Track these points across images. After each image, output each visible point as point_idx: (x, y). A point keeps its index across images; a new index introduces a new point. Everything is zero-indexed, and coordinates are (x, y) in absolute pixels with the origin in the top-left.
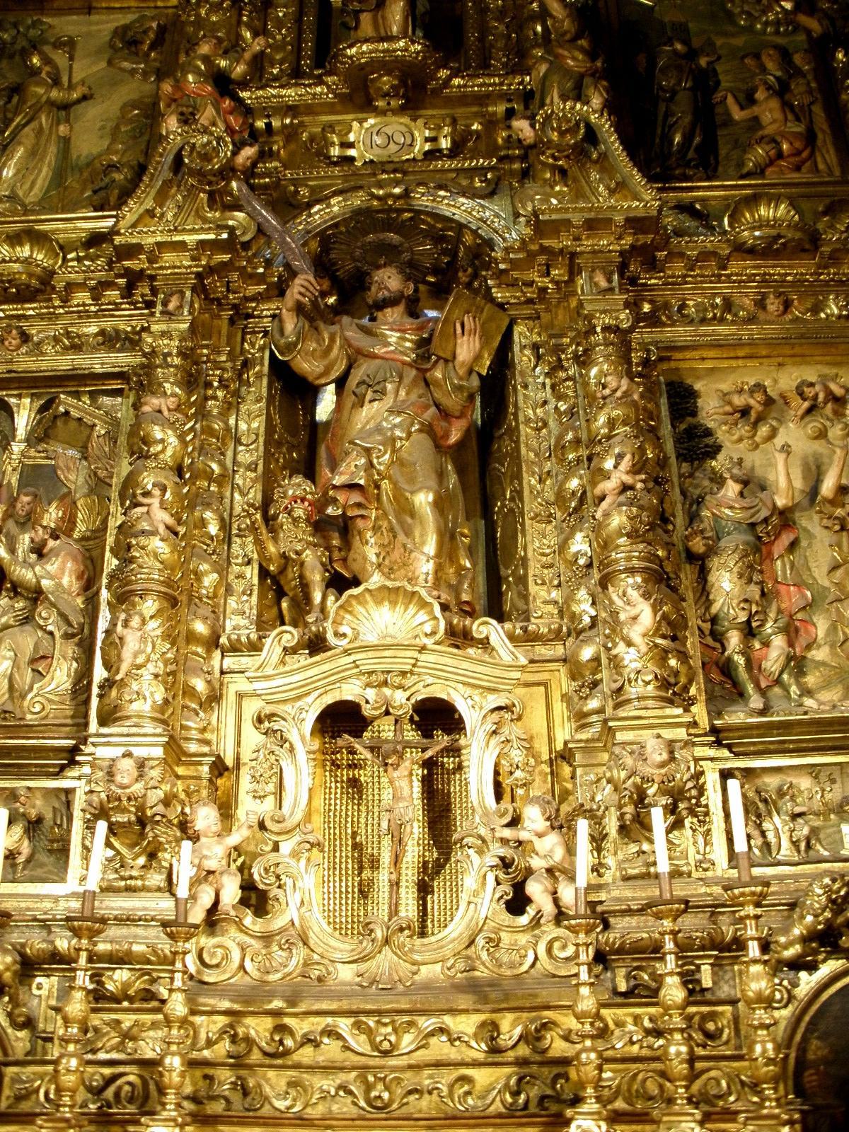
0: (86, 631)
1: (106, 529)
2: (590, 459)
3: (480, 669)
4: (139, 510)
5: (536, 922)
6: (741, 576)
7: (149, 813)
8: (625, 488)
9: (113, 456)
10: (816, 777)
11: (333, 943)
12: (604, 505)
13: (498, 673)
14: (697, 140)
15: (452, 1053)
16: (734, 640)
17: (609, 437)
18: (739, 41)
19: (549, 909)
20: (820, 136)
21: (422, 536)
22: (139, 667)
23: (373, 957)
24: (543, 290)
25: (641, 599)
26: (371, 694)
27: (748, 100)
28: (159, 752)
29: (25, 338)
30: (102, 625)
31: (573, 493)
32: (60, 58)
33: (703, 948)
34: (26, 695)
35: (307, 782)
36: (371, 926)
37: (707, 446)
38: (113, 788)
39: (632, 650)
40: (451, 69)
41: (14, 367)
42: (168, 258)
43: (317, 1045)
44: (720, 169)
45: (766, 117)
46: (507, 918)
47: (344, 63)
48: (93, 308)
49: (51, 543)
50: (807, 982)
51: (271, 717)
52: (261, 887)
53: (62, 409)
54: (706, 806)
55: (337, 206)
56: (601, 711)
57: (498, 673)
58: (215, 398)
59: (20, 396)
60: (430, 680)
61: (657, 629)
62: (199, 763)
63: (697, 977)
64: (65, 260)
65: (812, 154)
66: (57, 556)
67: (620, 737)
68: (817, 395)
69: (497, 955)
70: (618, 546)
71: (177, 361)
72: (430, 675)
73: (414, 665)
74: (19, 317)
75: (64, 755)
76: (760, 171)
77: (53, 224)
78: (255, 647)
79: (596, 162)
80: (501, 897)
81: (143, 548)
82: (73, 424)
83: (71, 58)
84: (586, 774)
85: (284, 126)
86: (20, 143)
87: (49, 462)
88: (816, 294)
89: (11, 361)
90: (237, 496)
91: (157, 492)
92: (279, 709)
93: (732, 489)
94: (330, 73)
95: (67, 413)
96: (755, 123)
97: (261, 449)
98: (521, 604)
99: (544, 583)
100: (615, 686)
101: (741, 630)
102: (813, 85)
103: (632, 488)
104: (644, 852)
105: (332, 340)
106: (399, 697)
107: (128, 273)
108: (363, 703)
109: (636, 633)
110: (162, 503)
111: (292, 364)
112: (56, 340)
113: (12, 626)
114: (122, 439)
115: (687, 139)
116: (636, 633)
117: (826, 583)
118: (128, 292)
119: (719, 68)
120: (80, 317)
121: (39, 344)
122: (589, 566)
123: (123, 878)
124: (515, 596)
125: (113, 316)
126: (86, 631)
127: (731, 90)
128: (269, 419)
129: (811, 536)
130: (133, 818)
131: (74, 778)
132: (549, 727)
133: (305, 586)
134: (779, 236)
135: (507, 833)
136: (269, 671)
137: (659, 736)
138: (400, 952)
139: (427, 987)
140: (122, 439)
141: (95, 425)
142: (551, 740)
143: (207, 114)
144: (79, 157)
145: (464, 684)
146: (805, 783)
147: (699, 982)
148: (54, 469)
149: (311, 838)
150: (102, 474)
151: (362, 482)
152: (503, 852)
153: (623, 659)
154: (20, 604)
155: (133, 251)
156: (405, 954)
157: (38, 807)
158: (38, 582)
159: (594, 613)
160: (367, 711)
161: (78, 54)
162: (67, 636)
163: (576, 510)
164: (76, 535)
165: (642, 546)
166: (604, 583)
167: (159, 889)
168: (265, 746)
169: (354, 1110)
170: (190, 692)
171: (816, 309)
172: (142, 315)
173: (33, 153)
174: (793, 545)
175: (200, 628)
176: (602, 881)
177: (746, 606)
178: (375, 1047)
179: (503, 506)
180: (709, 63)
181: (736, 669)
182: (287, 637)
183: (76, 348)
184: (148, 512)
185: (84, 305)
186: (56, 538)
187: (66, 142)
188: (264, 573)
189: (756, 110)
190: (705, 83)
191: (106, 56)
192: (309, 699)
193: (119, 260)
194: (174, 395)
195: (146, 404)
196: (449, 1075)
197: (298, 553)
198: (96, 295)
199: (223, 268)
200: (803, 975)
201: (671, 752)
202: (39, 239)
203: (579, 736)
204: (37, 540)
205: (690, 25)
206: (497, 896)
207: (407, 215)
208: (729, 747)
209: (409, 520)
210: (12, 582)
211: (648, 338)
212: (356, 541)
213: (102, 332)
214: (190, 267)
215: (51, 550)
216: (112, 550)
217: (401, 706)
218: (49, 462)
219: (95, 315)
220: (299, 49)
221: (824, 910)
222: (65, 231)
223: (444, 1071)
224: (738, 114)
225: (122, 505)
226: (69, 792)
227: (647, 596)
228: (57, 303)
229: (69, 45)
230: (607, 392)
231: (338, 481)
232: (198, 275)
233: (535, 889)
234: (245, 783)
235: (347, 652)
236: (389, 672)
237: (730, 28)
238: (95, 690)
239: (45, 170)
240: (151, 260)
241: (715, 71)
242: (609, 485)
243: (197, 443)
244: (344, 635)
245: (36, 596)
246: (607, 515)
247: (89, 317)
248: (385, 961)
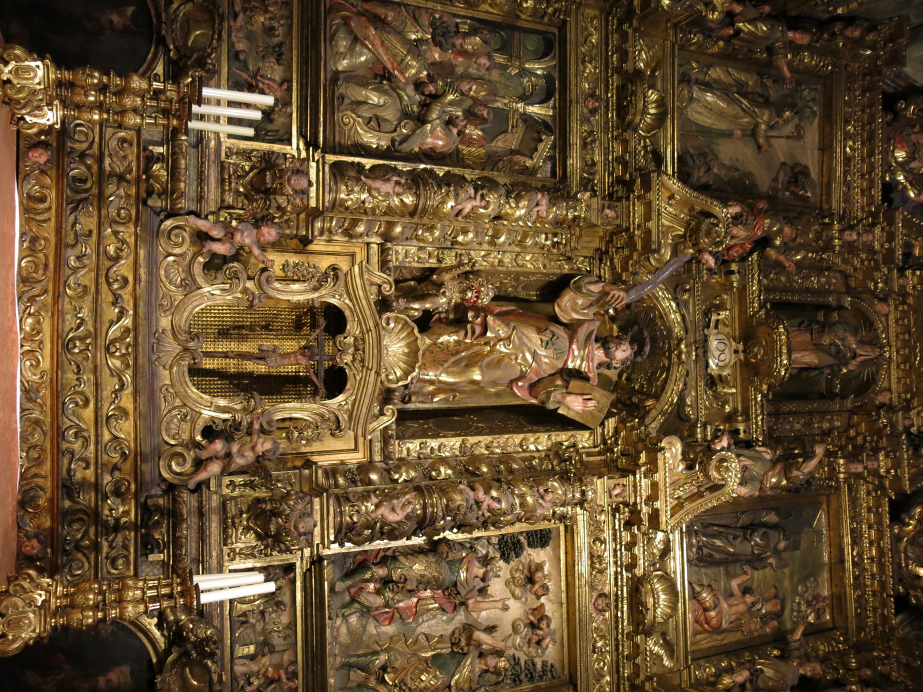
0: (397, 154)
1: (464, 167)
2: (499, 481)
3: (364, 410)
4: (472, 192)
5: (197, 445)
6: (423, 576)
7: (271, 197)
9: (512, 172)
10: (288, 627)
11: (186, 314)
12: (468, 490)
13: (362, 421)
14: (717, 556)
15: (106, 393)
16: (381, 572)
18: (786, 583)
19: (204, 455)
20: (720, 637)
21: (453, 372)
22: (369, 192)
23: (175, 340)
25: (405, 514)
26: (350, 340)
28: (313, 203)
29: (593, 111)
30: (401, 165)
31: (478, 469)
32: (789, 129)
33: (174, 555)
34: (354, 113)
35: (296, 298)
36: (196, 339)
37: (509, 554)
38: (289, 174)
39: (373, 507)
40: (768, 394)
41: (574, 105)
42: (639, 209)
43: (114, 304)
44: (696, 569)
46: (200, 425)
47: (773, 322)
48: (610, 157)
49: (455, 131)
50: (151, 624)
51: (336, 277)
52: (225, 268)
53: (544, 137)
54: (271, 555)
55: (675, 317)
56: (337, 485)
57: (362, 421)
58: (546, 239)
59: (554, 108)
60: (358, 378)
61: (386, 524)
62: (307, 230)
63: (156, 551)
64: (645, 138)
65: (706, 631)
66: (446, 135)
67: (317, 501)
68: (541, 629)
69: (175, 420)
70: (441, 499)
71: (570, 216)
72: (361, 378)
73: (368, 368)
74: (607, 107)
75: (313, 139)
77: (671, 129)
78: (384, 265)
80: (214, 423)
81: (447, 194)
82: (533, 146)
83: (788, 137)
84: (295, 477)
85: (732, 283)
86: (728, 104)
87: (510, 128)
89: (577, 102)
90: (483, 253)
91: (483, 203)
92: (341, 282)
94: (767, 314)
95: (541, 141)
97: (513, 269)
98: (409, 432)
99: (421, 448)
100: (351, 496)
101: (387, 576)
102: (756, 634)
103: (479, 508)
104: (241, 515)
105: (583, 314)
106: (348, 359)
107: (633, 181)
108: (345, 335)
109: (384, 511)
110: (476, 206)
111: (568, 290)
112: (591, 133)
113: (401, 103)
114: (522, 178)
115: (718, 549)
116: (384, 511)
118: (620, 181)
119: (768, 570)
120: (605, 148)
121: (589, 121)
122: (431, 478)
123: (230, 176)
124: (415, 429)
125: (605, 171)
126: (397, 154)
127: (752, 578)
128: (533, 274)
130: (268, 186)
131: (298, 145)
132: (328, 451)
133: (422, 297)
135: (256, 426)
136: (366, 276)
137: (315, 526)
138: (179, 358)
139: (154, 375)
140: (522, 178)
141: (532, 159)
142: (320, 453)
143: (740, 232)
144: (718, 144)
145: (355, 400)
146: (285, 619)
147: (152, 552)
148: (505, 132)
149: (256, 301)
150: (500, 165)
151: (489, 334)
152: (245, 423)
153: (368, 502)
154: (415, 109)
155: (647, 186)
156: (177, 361)
157: (279, 120)
158: (429, 122)
160: (340, 338)
161: (791, 142)
162: (393, 140)
163: (467, 470)
164: (460, 146)
165: (441, 514)
166: (418, 489)
167: (223, 201)
168: (318, 272)
169: (67, 329)
170: (355, 223)
172: (605, 190)
173: (721, 114)
175: (398, 229)
176: (224, 488)
177: (402, 580)
178: (113, 342)
179: (473, 421)
180: (771, 564)
182: (387, 287)
183: (584, 145)
184: (470, 198)
185: (613, 152)
186: (459, 134)
187: (729, 135)
188: (432, 271)
190: (756, 561)
191: (789, 162)
192: (347, 301)
193: (641, 176)
194: (548, 216)
195: (543, 195)
196: (89, 390)
197: (444, 293)
198: (620, 160)
199: (631, 244)
200: (155, 620)
201: (305, 534)
202: (660, 119)
203: (320, 472)
204: (457, 121)
205: (798, 552)
206: (216, 421)
207: (667, 363)
208: (309, 570)
209: (463, 364)
210: (430, 104)
211: (580, 518)
212: (451, 329)
213: (594, 164)
214: (634, 223)
215: (451, 131)
216: (449, 172)
217: (341, 359)
218: (510, 128)
219: (607, 159)
220: (787, 291)
221: (196, 636)
222: (665, 137)
223: (92, 388)
224: (735, 584)
225: (479, 179)
226: (289, 142)
227: (408, 517)
228: (615, 133)
229: (798, 135)
231: (490, 319)
232: (628, 229)
233: (219, 446)
234: (293, 259)
235: (377, 325)
236: (364, 351)
237: (796, 579)
238: (357, 160)
239: (710, 121)
240: (639, 197)
241: (766, 567)
243: (519, 228)
244: (388, 324)
245: (421, 120)
246: (461, 492)
247: (605, 155)
248: (171, 347)
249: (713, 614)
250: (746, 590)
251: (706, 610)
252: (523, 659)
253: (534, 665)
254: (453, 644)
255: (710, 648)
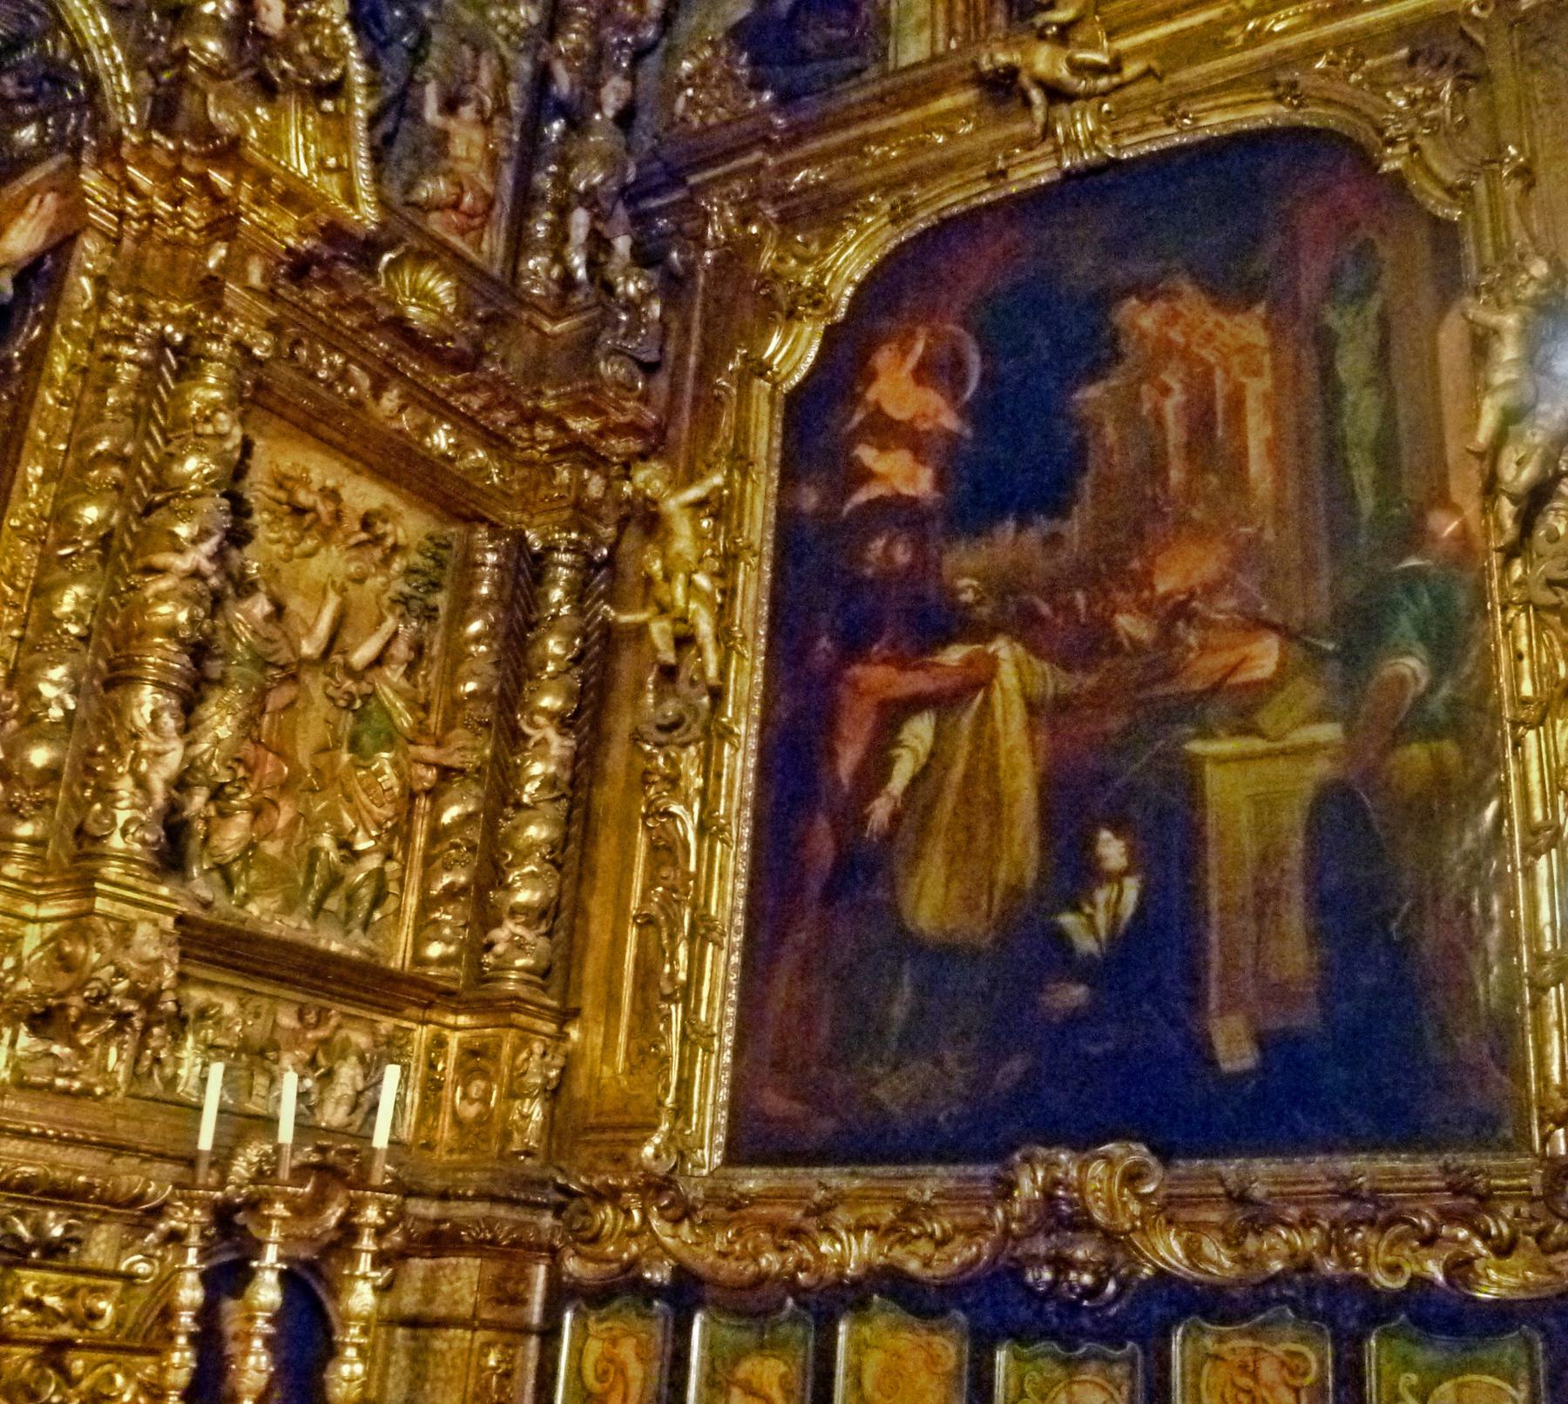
8: (196, 574)
17: (197, 495)
24: (150, 216)
27: (450, 105)
45: (458, 148)
65: (482, 226)
76: (425, 208)
79: (324, 114)
88: (432, 411)
93: (260, 606)
96: (442, 139)
117: (307, 766)
129: (310, 701)
134: (452, 339)
159: (71, 705)
171: (426, 430)
174: (291, 705)
181: (190, 836)
189: (452, 125)
230: (209, 429)
242: (183, 563)
249: (468, 199)
250: (450, 105)
251: (455, 206)
252: (400, 586)
253: (415, 572)
254: (348, 707)
255: (508, 239)
